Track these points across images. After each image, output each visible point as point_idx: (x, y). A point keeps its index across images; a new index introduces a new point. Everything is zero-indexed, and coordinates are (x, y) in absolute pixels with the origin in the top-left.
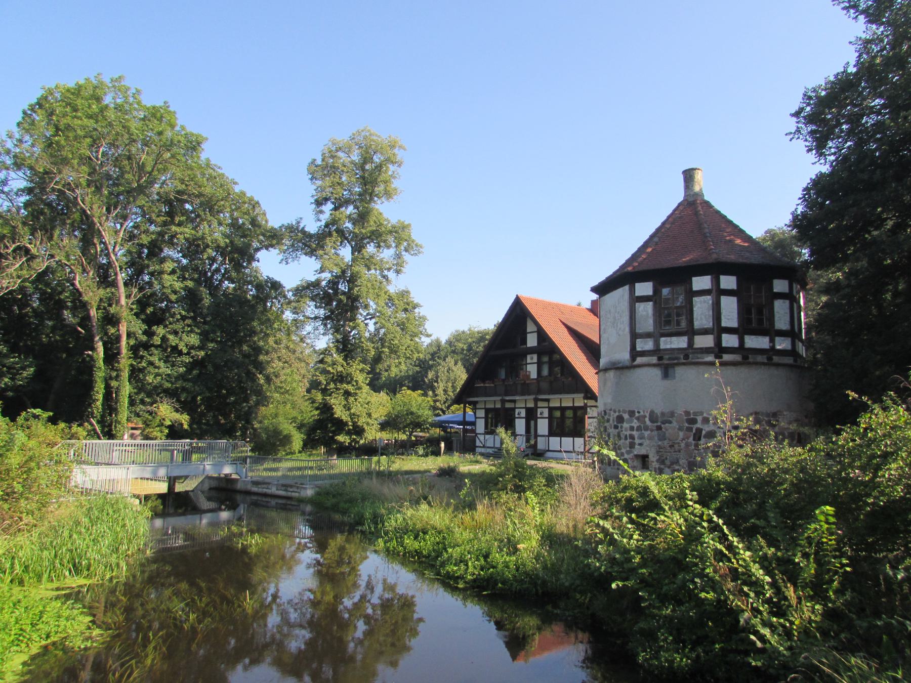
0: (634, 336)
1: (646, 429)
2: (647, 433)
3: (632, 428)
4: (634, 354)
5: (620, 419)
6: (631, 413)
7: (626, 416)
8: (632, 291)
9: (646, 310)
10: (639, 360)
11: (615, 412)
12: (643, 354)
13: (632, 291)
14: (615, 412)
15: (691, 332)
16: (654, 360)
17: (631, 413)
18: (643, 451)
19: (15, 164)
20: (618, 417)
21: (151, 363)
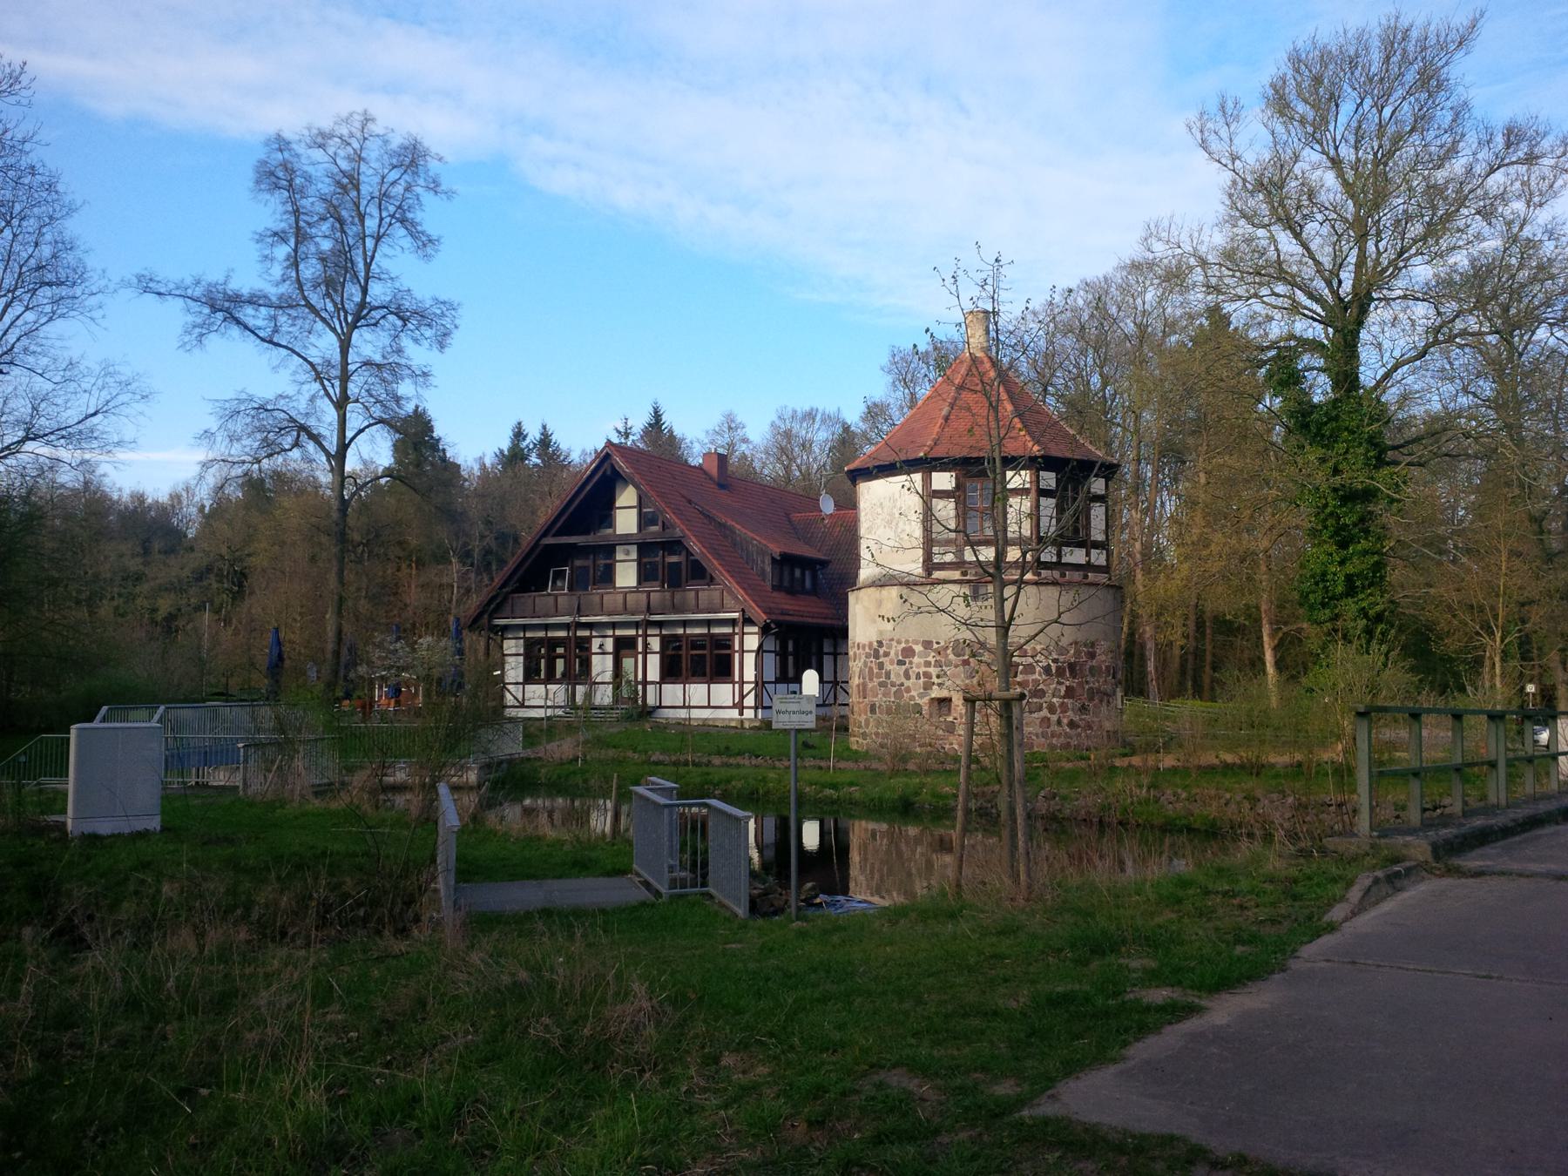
0: (929, 542)
1: (949, 664)
2: (949, 671)
3: (928, 664)
4: (929, 565)
5: (909, 652)
6: (927, 644)
7: (918, 648)
8: (927, 481)
9: (946, 510)
10: (937, 575)
11: (899, 642)
12: (942, 566)
13: (927, 481)
14: (899, 642)
15: (1001, 542)
16: (956, 575)
17: (927, 644)
18: (944, 694)
19: (1093, 952)
20: (904, 650)
21: (103, 920)
